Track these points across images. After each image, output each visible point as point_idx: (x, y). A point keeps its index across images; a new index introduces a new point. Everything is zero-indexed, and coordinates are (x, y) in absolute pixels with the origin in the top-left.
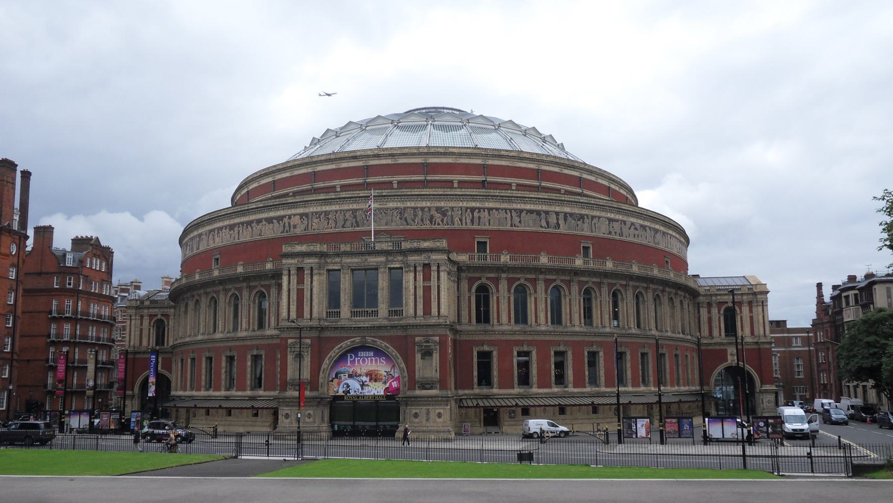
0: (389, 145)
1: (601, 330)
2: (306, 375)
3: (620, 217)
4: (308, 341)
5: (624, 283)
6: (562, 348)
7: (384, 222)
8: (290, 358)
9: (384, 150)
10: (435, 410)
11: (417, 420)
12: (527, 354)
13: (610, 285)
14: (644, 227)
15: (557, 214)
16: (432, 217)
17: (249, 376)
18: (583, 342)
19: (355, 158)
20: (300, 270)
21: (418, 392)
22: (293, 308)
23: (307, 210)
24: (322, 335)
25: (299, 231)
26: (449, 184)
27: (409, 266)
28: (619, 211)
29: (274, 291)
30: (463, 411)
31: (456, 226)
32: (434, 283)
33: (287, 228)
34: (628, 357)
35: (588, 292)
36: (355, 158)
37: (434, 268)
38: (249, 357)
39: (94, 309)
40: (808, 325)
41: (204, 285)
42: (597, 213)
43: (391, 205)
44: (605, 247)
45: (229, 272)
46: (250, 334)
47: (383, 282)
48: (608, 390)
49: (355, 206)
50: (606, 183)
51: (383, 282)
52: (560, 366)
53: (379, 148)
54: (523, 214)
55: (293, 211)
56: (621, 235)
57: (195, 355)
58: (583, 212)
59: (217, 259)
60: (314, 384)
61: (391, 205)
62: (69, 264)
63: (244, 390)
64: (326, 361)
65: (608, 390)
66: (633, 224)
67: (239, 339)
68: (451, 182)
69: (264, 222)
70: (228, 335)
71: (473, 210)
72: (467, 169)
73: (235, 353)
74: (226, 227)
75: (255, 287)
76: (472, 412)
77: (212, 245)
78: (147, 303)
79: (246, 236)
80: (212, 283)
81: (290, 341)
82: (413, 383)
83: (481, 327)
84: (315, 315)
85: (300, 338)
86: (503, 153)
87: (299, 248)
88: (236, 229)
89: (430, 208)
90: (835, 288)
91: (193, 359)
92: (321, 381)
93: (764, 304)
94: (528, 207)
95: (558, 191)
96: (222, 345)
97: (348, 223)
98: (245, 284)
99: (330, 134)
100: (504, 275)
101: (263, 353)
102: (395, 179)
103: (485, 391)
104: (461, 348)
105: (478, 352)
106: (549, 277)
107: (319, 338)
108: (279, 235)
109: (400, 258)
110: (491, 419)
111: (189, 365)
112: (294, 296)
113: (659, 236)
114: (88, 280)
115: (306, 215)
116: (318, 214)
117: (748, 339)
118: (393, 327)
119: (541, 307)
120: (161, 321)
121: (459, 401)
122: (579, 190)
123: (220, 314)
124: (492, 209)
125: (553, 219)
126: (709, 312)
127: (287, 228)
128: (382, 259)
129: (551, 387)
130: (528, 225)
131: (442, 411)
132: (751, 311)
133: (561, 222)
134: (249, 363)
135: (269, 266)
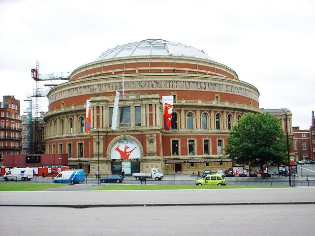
0: (134, 55)
1: (224, 131)
2: (101, 151)
3: (231, 84)
4: (102, 137)
5: (233, 111)
6: (207, 139)
7: (132, 87)
8: (95, 144)
9: (132, 57)
10: (155, 164)
11: (147, 169)
12: (193, 141)
13: (227, 113)
14: (241, 88)
15: (205, 83)
16: (152, 85)
17: (77, 152)
18: (216, 136)
20: (98, 107)
21: (148, 157)
22: (95, 123)
23: (100, 83)
24: (108, 134)
25: (97, 92)
26: (160, 71)
27: (143, 105)
28: (231, 82)
30: (167, 164)
31: (163, 89)
32: (154, 112)
33: (92, 90)
35: (218, 115)
36: (120, 60)
37: (154, 106)
38: (77, 144)
39: (13, 126)
40: (308, 128)
43: (135, 80)
44: (225, 97)
45: (69, 109)
46: (79, 134)
47: (133, 110)
49: (120, 81)
50: (225, 70)
51: (133, 110)
53: (130, 56)
54: (191, 83)
56: (231, 92)
57: (55, 144)
58: (216, 82)
59: (63, 104)
60: (105, 155)
61: (135, 80)
62: (2, 106)
63: (76, 157)
64: (109, 145)
66: (236, 87)
67: (72, 137)
68: (161, 70)
69: (82, 88)
70: (69, 135)
71: (170, 81)
72: (167, 65)
73: (71, 143)
76: (170, 165)
77: (61, 98)
79: (75, 94)
81: (94, 137)
82: (145, 153)
83: (174, 130)
84: (104, 126)
85: (98, 136)
86: (182, 58)
88: (71, 91)
89: (151, 81)
91: (54, 145)
92: (107, 153)
93: (290, 119)
94: (193, 80)
95: (205, 74)
97: (118, 88)
98: (75, 114)
99: (109, 50)
100: (183, 109)
101: (83, 142)
102: (137, 69)
103: (176, 157)
104: (165, 139)
105: (173, 141)
106: (201, 109)
107: (106, 135)
108: (89, 93)
109: (140, 102)
110: (178, 167)
111: (53, 148)
113: (247, 92)
114: (10, 114)
115: (100, 84)
118: (137, 131)
119: (198, 121)
121: (165, 160)
122: (214, 73)
123: (65, 126)
124: (178, 81)
125: (203, 86)
127: (92, 90)
129: (202, 154)
130: (193, 88)
131: (158, 165)
134: (77, 147)
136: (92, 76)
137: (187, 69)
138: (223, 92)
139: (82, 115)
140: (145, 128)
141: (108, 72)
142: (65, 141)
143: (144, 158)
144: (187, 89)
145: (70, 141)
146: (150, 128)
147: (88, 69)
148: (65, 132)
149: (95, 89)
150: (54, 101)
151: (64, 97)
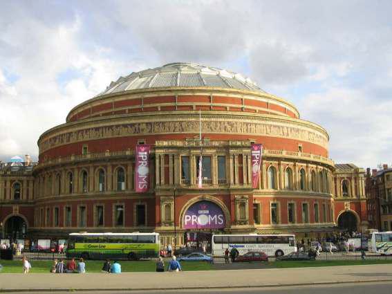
6: (292, 202)
8: (163, 207)
14: (320, 136)
15: (287, 128)
16: (226, 127)
19: (170, 91)
23: (150, 121)
25: (146, 133)
29: (130, 168)
31: (239, 132)
34: (318, 207)
36: (170, 91)
37: (244, 157)
41: (77, 163)
42: (304, 128)
43: (201, 119)
45: (98, 156)
46: (114, 193)
48: (312, 224)
49: (181, 120)
50: (293, 111)
52: (291, 212)
55: (141, 121)
59: (85, 148)
65: (312, 224)
67: (106, 196)
71: (247, 124)
72: (233, 100)
73: (103, 205)
74: (92, 129)
75: (117, 165)
77: (81, 139)
78: (9, 173)
79: (108, 135)
80: (85, 162)
87: (165, 143)
88: (101, 131)
90: (374, 171)
96: (92, 199)
98: (109, 164)
101: (123, 204)
102: (194, 104)
109: (224, 150)
112: (162, 169)
115: (150, 123)
116: (158, 123)
117: (355, 197)
120: (18, 184)
125: (285, 131)
126: (335, 183)
128: (214, 151)
129: (287, 223)
130: (275, 133)
132: (356, 182)
133: (289, 132)
135: (128, 153)
136: (124, 112)
137: (257, 109)
138: (306, 141)
139: (121, 165)
140: (232, 187)
141: (152, 105)
142: (90, 203)
143: (233, 227)
144: (268, 135)
145: (101, 202)
146: (240, 187)
147: (117, 100)
148: (91, 189)
149: (143, 130)
150: (65, 143)
151: (88, 139)
